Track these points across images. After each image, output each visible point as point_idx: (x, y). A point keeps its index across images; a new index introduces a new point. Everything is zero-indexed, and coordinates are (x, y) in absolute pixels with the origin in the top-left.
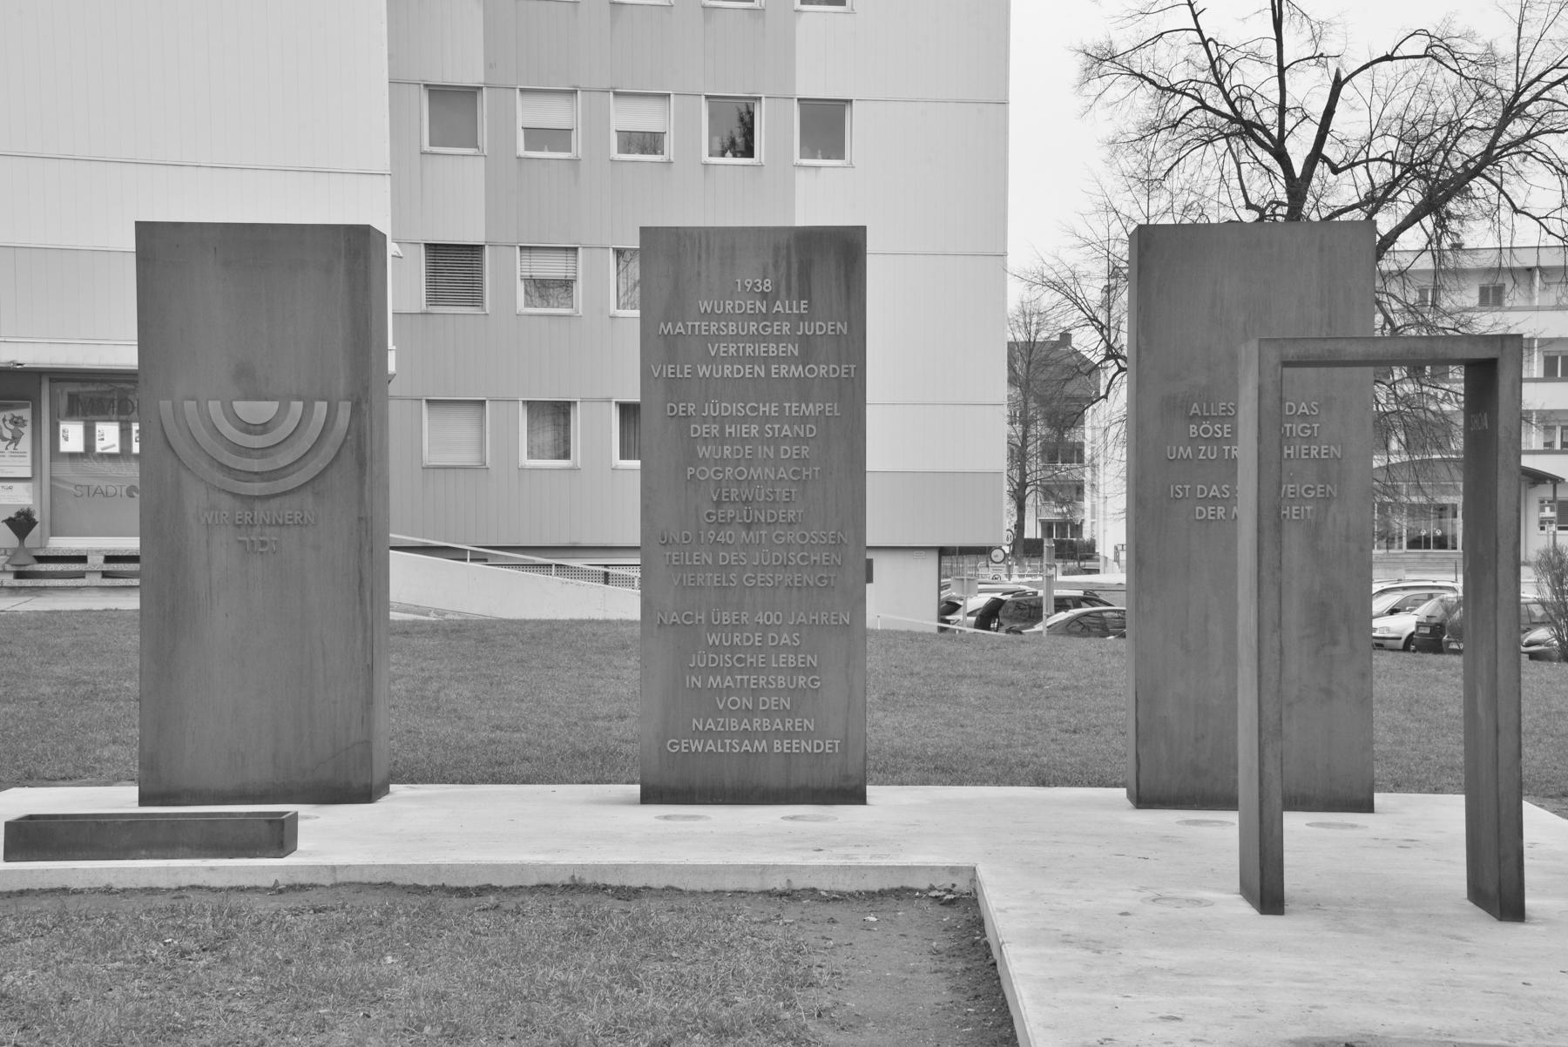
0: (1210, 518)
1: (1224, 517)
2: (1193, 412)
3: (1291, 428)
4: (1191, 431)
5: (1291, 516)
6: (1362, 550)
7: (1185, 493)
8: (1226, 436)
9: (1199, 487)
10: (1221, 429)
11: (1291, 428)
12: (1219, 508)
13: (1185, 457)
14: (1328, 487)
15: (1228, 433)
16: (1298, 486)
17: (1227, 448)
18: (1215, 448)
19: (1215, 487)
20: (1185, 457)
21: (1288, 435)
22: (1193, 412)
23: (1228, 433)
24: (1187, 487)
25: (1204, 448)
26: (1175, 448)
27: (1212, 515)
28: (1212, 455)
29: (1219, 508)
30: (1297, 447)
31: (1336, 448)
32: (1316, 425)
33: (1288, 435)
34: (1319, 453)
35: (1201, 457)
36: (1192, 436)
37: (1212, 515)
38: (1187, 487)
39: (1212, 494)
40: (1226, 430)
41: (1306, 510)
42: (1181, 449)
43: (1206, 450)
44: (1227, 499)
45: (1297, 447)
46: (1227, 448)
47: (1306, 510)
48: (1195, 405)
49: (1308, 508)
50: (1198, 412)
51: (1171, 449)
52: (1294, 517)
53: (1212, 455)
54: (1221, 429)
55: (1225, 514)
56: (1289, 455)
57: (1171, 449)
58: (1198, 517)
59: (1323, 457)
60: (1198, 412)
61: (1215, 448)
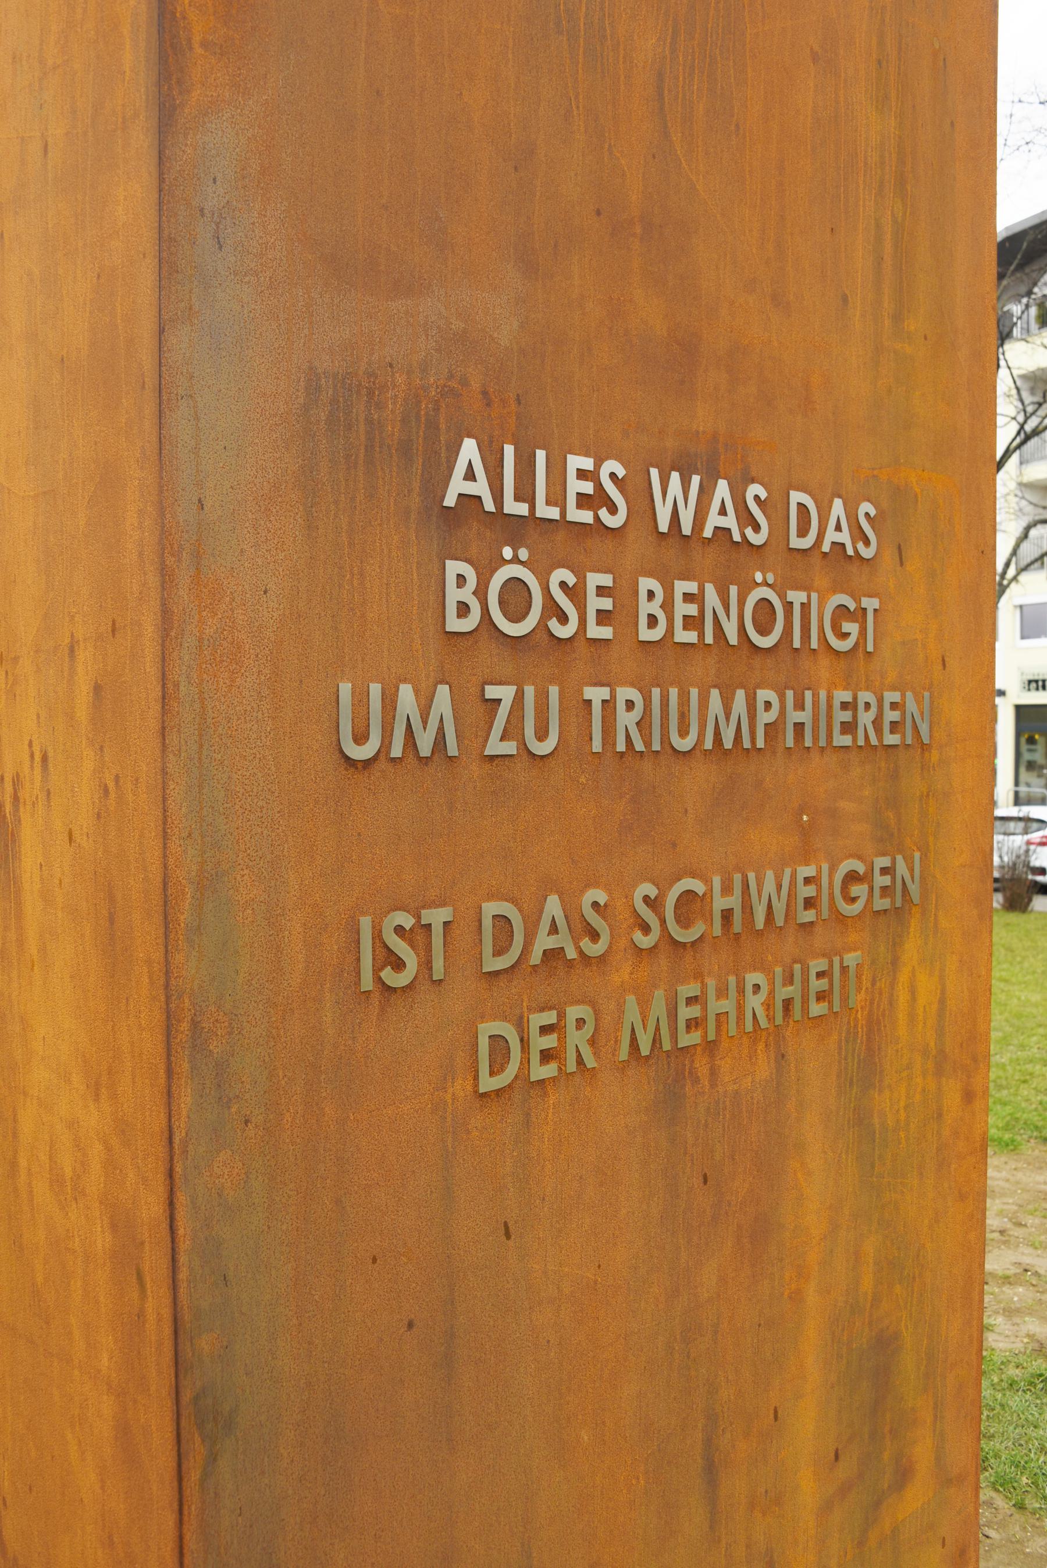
0: (541, 1072)
1: (590, 1062)
2: (457, 486)
3: (805, 607)
4: (454, 595)
5: (805, 1001)
6: (969, 1096)
7: (427, 964)
8: (595, 631)
9: (491, 908)
10: (576, 593)
11: (805, 607)
12: (574, 1012)
13: (425, 744)
14: (901, 868)
15: (603, 617)
16: (825, 867)
17: (597, 694)
18: (554, 691)
19: (553, 906)
20: (425, 744)
21: (797, 644)
22: (457, 486)
23: (603, 617)
24: (436, 917)
25: (505, 693)
26: (375, 689)
27: (546, 1056)
28: (542, 735)
29: (574, 1012)
30: (823, 695)
31: (919, 700)
32: (870, 604)
33: (797, 644)
34: (877, 723)
35: (496, 746)
36: (455, 624)
37: (546, 1056)
38: (436, 917)
39: (544, 942)
40: (595, 603)
41: (844, 969)
42: (406, 694)
43: (519, 697)
44: (602, 959)
45: (823, 695)
46: (597, 694)
47: (844, 969)
48: (469, 450)
49: (851, 959)
50: (480, 487)
51: (361, 699)
52: (817, 1009)
53: (542, 735)
54: (576, 593)
55: (592, 1042)
56: (799, 727)
57: (361, 699)
58: (488, 1083)
59: (891, 739)
60: (480, 487)
61: (554, 691)
